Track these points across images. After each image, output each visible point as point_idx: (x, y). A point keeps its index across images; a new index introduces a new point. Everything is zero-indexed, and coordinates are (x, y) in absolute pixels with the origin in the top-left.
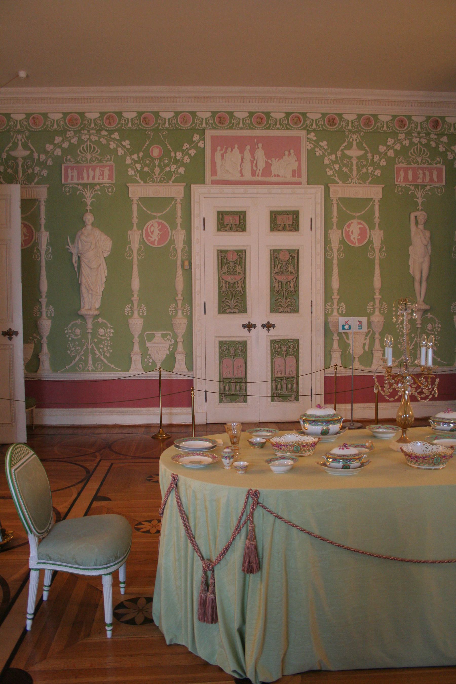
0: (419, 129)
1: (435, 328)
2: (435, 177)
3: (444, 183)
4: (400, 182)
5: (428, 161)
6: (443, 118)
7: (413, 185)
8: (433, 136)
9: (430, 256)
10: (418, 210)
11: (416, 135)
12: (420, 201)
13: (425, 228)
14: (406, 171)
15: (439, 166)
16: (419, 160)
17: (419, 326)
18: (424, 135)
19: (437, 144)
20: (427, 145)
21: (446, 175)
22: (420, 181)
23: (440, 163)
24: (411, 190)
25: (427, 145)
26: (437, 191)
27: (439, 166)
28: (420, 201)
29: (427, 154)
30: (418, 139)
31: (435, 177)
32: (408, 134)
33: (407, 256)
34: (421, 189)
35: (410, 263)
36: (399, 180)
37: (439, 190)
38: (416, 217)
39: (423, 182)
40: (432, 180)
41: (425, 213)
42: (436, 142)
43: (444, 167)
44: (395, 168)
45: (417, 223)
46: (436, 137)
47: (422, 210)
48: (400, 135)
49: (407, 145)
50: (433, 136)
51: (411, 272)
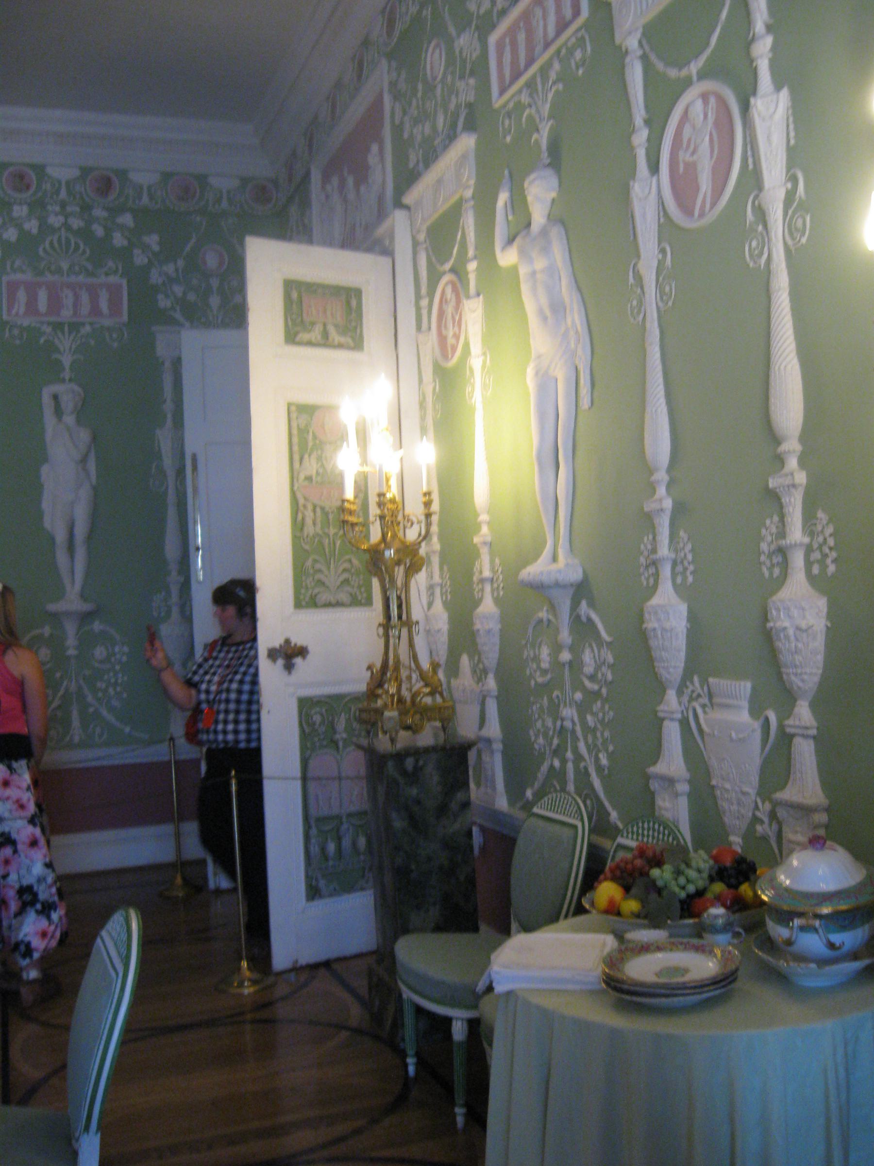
0: (63, 194)
1: (114, 654)
2: (104, 306)
3: (125, 318)
4: (17, 314)
5: (87, 270)
6: (122, 174)
7: (49, 324)
8: (98, 212)
9: (95, 489)
10: (63, 381)
11: (58, 209)
12: (67, 360)
13: (79, 422)
14: (32, 290)
15: (112, 279)
16: (65, 266)
17: (72, 652)
18: (78, 209)
19: (108, 231)
20: (85, 234)
21: (129, 301)
22: (66, 314)
23: (115, 272)
24: (44, 333)
25: (85, 234)
26: (111, 336)
27: (112, 279)
28: (67, 360)
29: (84, 252)
30: (61, 219)
31: (104, 306)
32: (38, 206)
33: (38, 488)
34: (70, 333)
35: (45, 505)
36: (14, 312)
37: (115, 336)
38: (56, 397)
39: (75, 314)
40: (95, 311)
41: (77, 388)
42: (105, 227)
43: (124, 282)
44: (4, 285)
45: (58, 412)
46: (105, 214)
47: (70, 380)
48: (16, 208)
49: (35, 231)
50: (98, 212)
51: (47, 525)
